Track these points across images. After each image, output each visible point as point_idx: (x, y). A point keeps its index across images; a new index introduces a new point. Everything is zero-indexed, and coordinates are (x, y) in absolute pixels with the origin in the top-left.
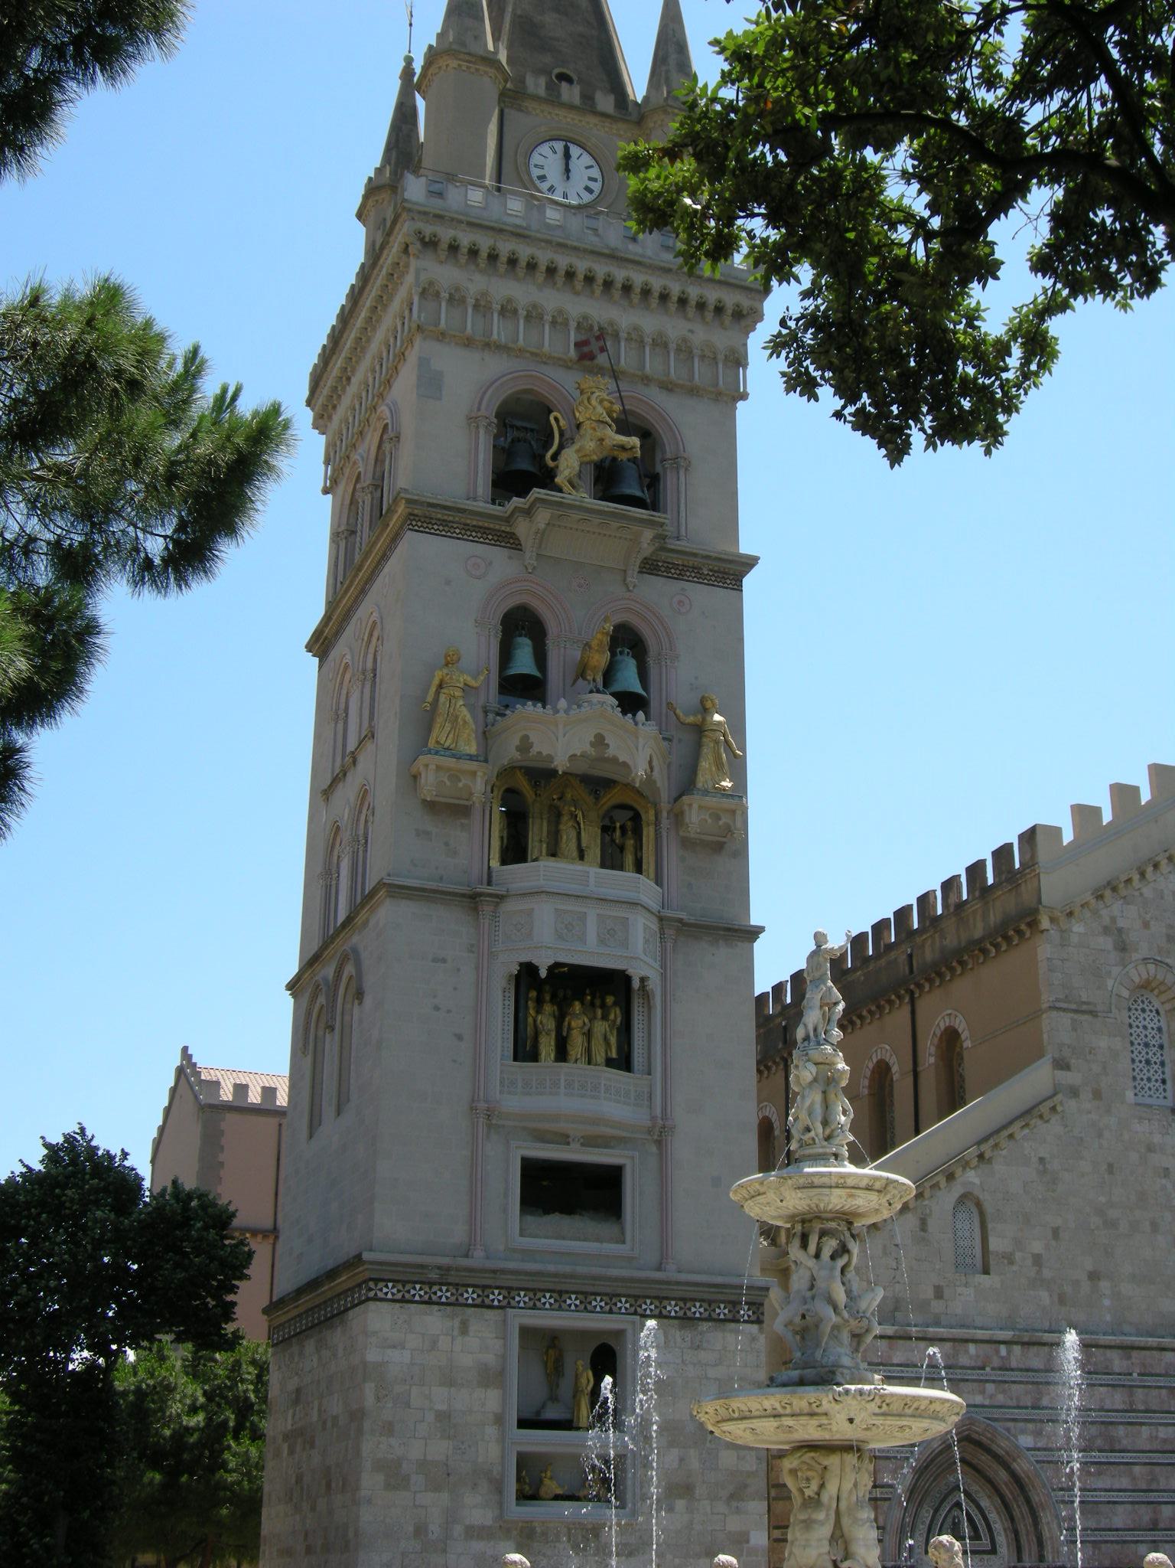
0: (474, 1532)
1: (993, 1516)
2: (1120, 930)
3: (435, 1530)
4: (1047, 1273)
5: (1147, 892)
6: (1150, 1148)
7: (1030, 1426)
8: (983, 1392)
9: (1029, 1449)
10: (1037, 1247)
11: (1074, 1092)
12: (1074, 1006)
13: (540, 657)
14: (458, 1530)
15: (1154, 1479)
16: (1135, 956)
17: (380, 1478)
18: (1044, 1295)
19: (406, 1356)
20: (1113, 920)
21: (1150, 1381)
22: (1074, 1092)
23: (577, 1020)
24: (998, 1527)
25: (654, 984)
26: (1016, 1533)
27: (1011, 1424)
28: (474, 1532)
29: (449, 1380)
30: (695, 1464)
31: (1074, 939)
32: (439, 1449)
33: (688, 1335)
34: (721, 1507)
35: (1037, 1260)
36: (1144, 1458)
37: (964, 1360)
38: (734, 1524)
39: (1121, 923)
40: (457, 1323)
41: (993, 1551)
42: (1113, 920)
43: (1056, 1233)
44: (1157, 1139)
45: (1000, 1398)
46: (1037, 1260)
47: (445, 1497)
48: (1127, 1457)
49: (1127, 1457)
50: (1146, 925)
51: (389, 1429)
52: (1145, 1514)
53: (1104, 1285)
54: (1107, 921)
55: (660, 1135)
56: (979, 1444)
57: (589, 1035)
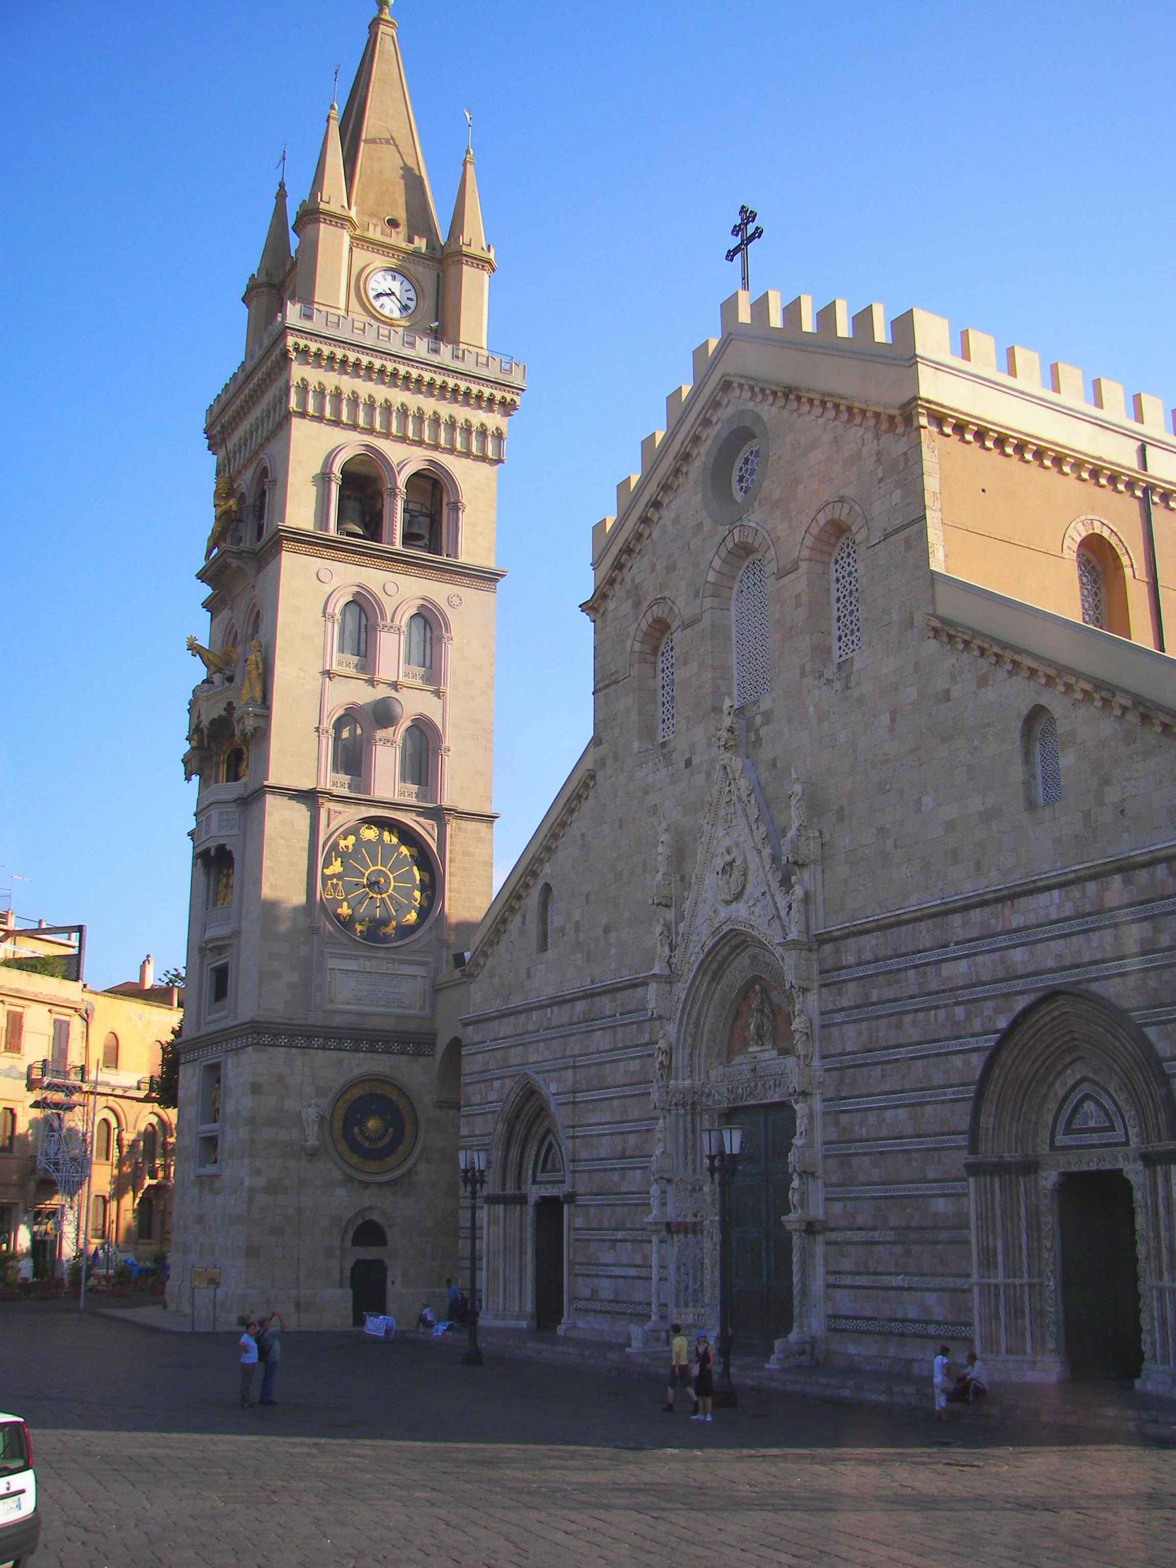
2: (637, 587)
7: (556, 1075)
8: (538, 1051)
9: (554, 1095)
10: (577, 916)
12: (607, 682)
16: (645, 605)
20: (633, 579)
21: (628, 1019)
27: (546, 1075)
31: (610, 616)
37: (531, 1027)
42: (633, 579)
50: (653, 569)
53: (613, 935)
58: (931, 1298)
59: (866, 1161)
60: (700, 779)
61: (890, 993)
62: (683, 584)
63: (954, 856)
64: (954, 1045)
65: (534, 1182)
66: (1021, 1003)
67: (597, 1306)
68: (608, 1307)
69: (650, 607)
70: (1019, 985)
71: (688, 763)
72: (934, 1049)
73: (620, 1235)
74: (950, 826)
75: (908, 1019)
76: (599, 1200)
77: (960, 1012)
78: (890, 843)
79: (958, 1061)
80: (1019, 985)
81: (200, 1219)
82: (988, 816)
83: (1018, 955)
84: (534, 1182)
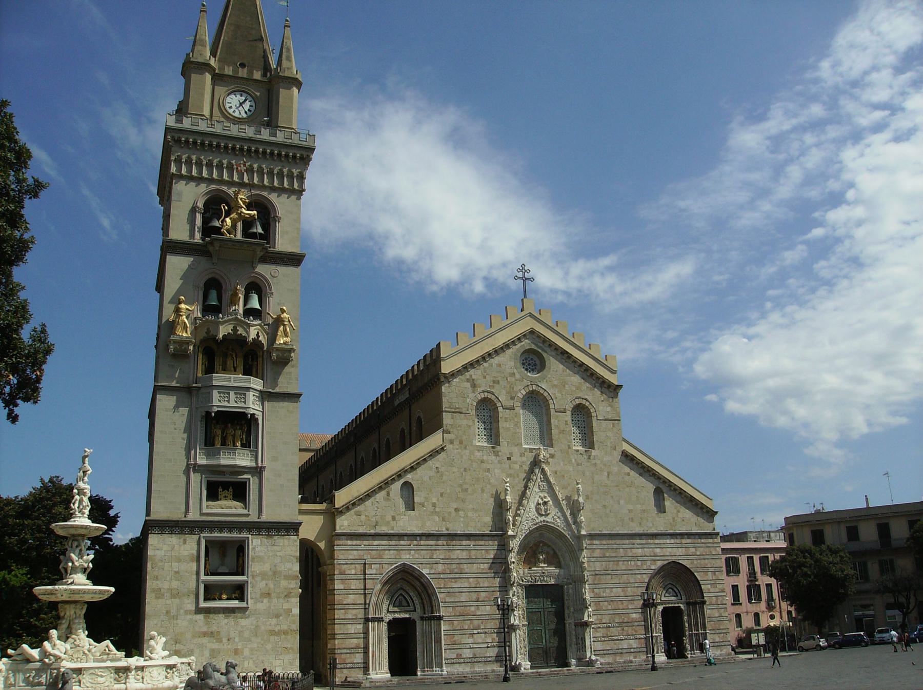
0: (186, 612)
1: (414, 598)
3: (173, 612)
4: (437, 509)
5: (486, 365)
6: (482, 462)
10: (434, 500)
11: (452, 442)
13: (220, 299)
14: (182, 611)
15: (478, 583)
17: (153, 595)
18: (437, 518)
19: (163, 553)
20: (471, 376)
22: (452, 442)
23: (230, 431)
24: (416, 602)
25: (259, 415)
26: (423, 604)
28: (186, 612)
29: (179, 560)
30: (272, 586)
32: (175, 584)
33: (270, 541)
34: (281, 600)
35: (434, 505)
36: (474, 576)
38: (286, 606)
39: (474, 377)
40: (182, 540)
41: (415, 611)
43: (442, 495)
44: (485, 458)
45: (417, 556)
46: (434, 505)
47: (176, 601)
48: (467, 576)
49: (467, 576)
50: (485, 377)
51: (157, 578)
52: (474, 596)
53: (461, 513)
54: (468, 377)
55: (258, 471)
56: (408, 573)
57: (234, 436)
58: (631, 642)
59: (606, 603)
60: (517, 467)
61: (614, 555)
62: (504, 392)
63: (632, 520)
64: (637, 572)
65: (388, 612)
66: (659, 564)
67: (462, 661)
68: (469, 660)
69: (483, 392)
70: (658, 558)
71: (509, 459)
72: (630, 572)
73: (475, 632)
74: (630, 511)
75: (621, 563)
76: (461, 618)
77: (639, 563)
78: (608, 511)
79: (639, 576)
80: (658, 558)
81: (211, 634)
82: (644, 511)
83: (658, 550)
84: (388, 612)
